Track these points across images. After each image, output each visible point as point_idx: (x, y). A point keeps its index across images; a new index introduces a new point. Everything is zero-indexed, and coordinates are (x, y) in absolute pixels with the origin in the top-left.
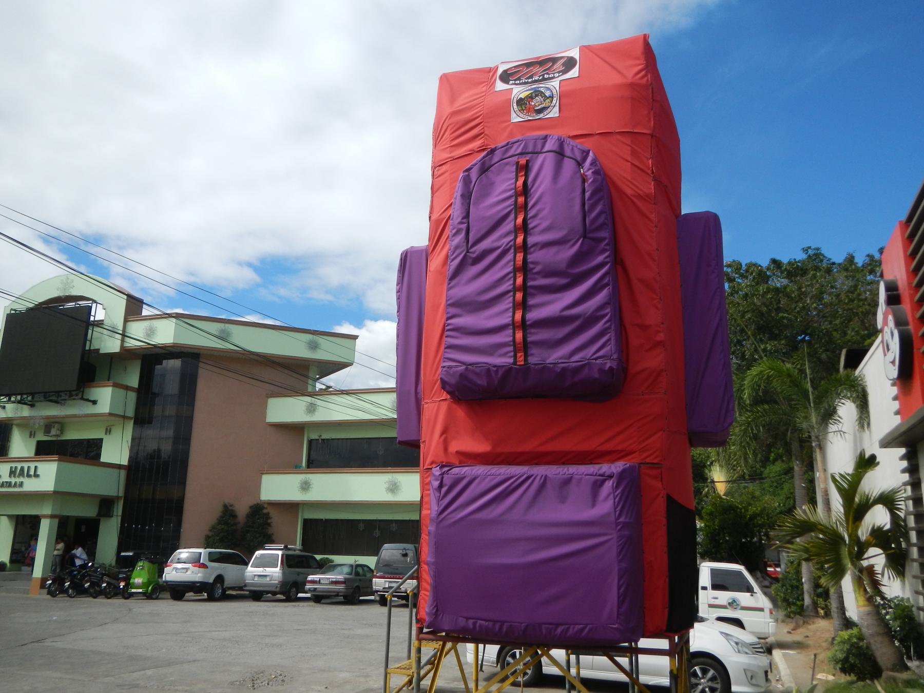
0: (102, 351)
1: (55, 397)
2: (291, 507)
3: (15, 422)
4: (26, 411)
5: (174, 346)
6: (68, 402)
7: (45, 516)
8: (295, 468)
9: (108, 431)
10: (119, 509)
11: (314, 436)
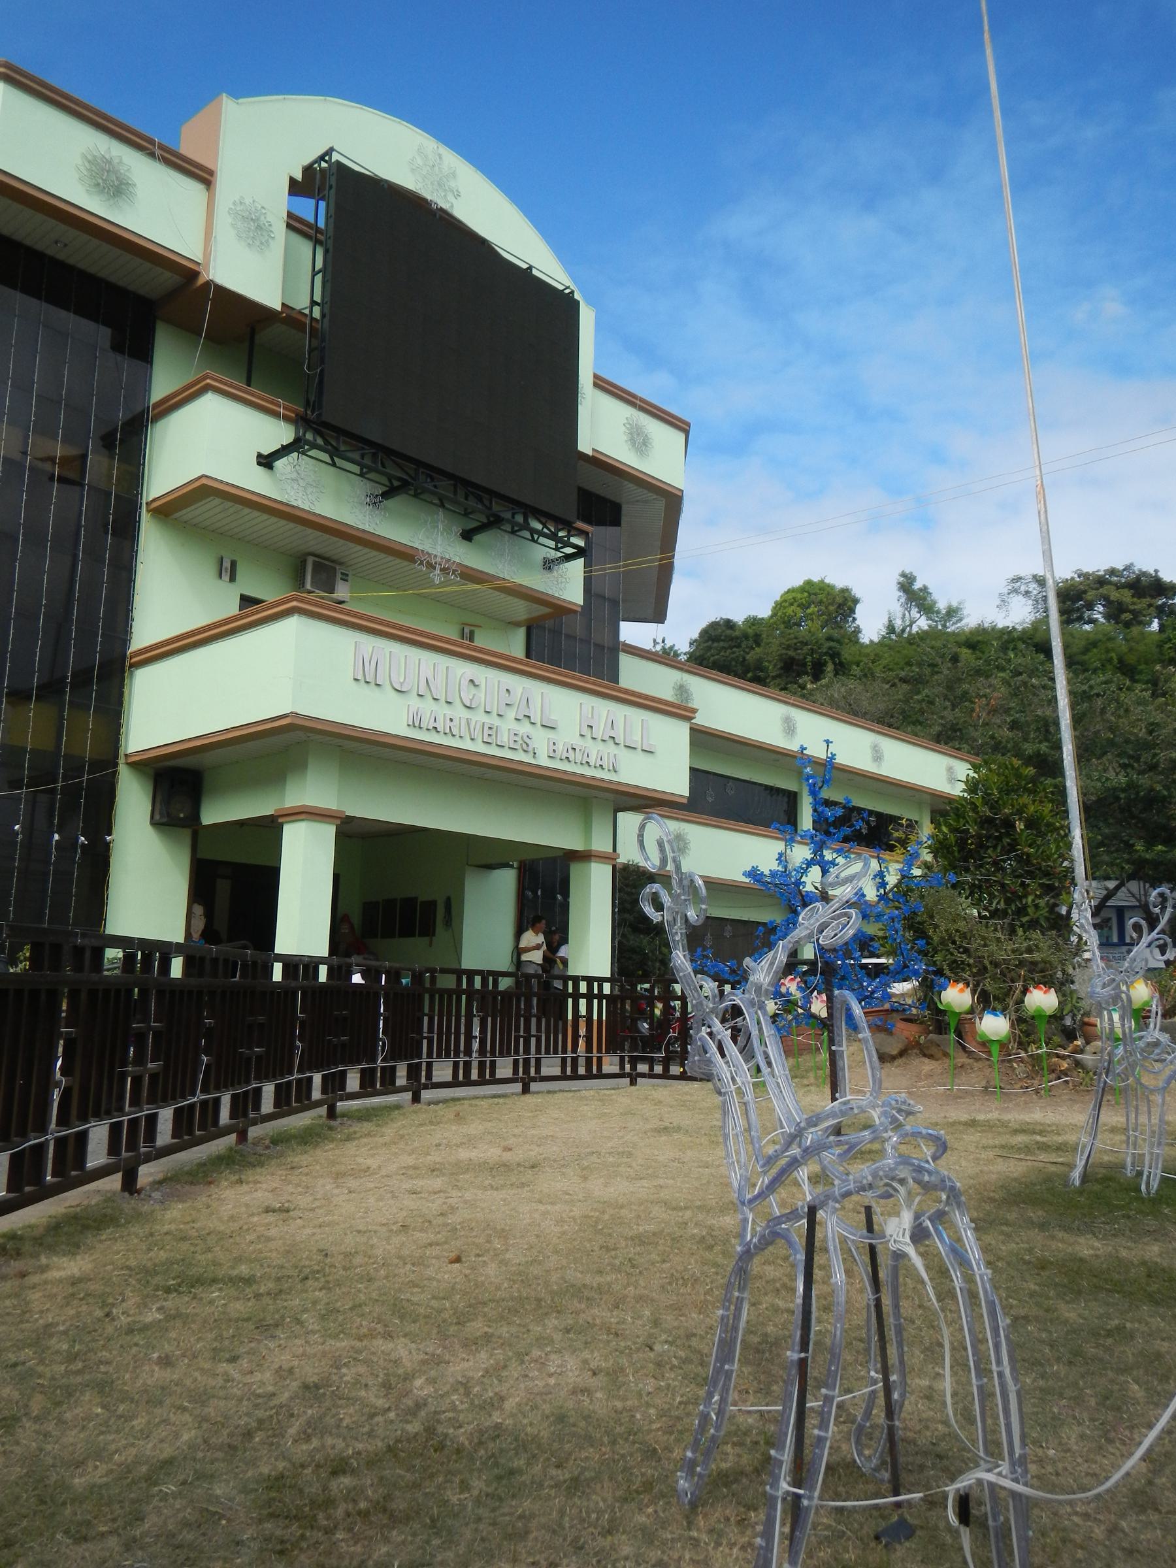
7: (602, 857)
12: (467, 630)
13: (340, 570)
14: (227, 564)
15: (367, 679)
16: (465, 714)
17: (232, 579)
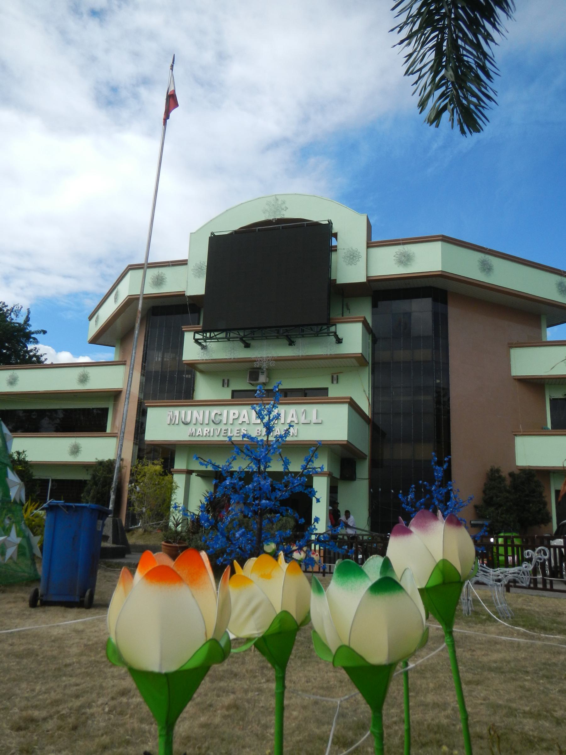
0: (338, 282)
1: (289, 333)
2: (546, 474)
3: (200, 367)
4: (240, 353)
5: (442, 276)
6: (299, 341)
8: (538, 430)
9: (335, 379)
10: (363, 471)
11: (559, 395)
12: (335, 376)
13: (260, 371)
14: (226, 381)
15: (172, 423)
16: (215, 427)
17: (228, 386)
